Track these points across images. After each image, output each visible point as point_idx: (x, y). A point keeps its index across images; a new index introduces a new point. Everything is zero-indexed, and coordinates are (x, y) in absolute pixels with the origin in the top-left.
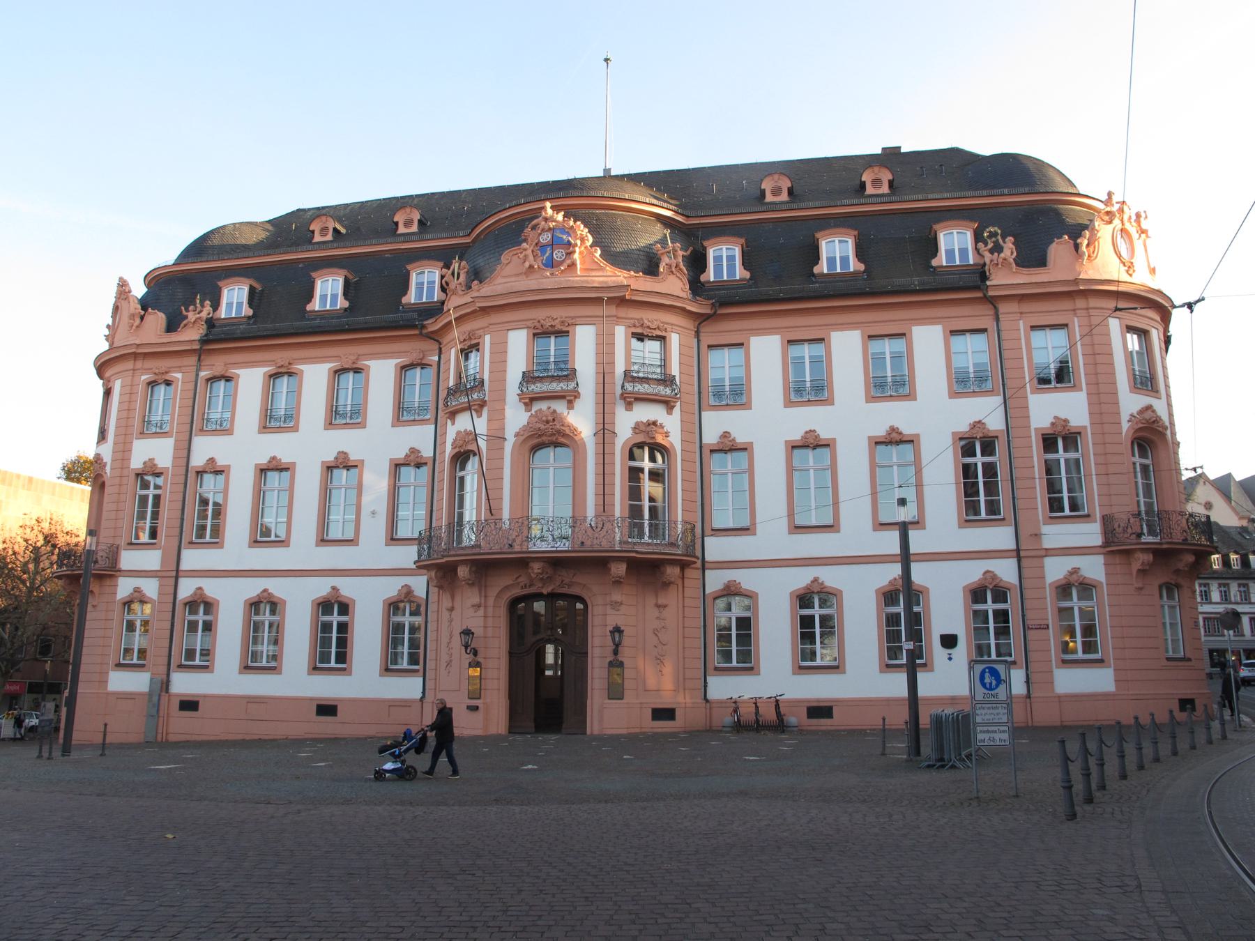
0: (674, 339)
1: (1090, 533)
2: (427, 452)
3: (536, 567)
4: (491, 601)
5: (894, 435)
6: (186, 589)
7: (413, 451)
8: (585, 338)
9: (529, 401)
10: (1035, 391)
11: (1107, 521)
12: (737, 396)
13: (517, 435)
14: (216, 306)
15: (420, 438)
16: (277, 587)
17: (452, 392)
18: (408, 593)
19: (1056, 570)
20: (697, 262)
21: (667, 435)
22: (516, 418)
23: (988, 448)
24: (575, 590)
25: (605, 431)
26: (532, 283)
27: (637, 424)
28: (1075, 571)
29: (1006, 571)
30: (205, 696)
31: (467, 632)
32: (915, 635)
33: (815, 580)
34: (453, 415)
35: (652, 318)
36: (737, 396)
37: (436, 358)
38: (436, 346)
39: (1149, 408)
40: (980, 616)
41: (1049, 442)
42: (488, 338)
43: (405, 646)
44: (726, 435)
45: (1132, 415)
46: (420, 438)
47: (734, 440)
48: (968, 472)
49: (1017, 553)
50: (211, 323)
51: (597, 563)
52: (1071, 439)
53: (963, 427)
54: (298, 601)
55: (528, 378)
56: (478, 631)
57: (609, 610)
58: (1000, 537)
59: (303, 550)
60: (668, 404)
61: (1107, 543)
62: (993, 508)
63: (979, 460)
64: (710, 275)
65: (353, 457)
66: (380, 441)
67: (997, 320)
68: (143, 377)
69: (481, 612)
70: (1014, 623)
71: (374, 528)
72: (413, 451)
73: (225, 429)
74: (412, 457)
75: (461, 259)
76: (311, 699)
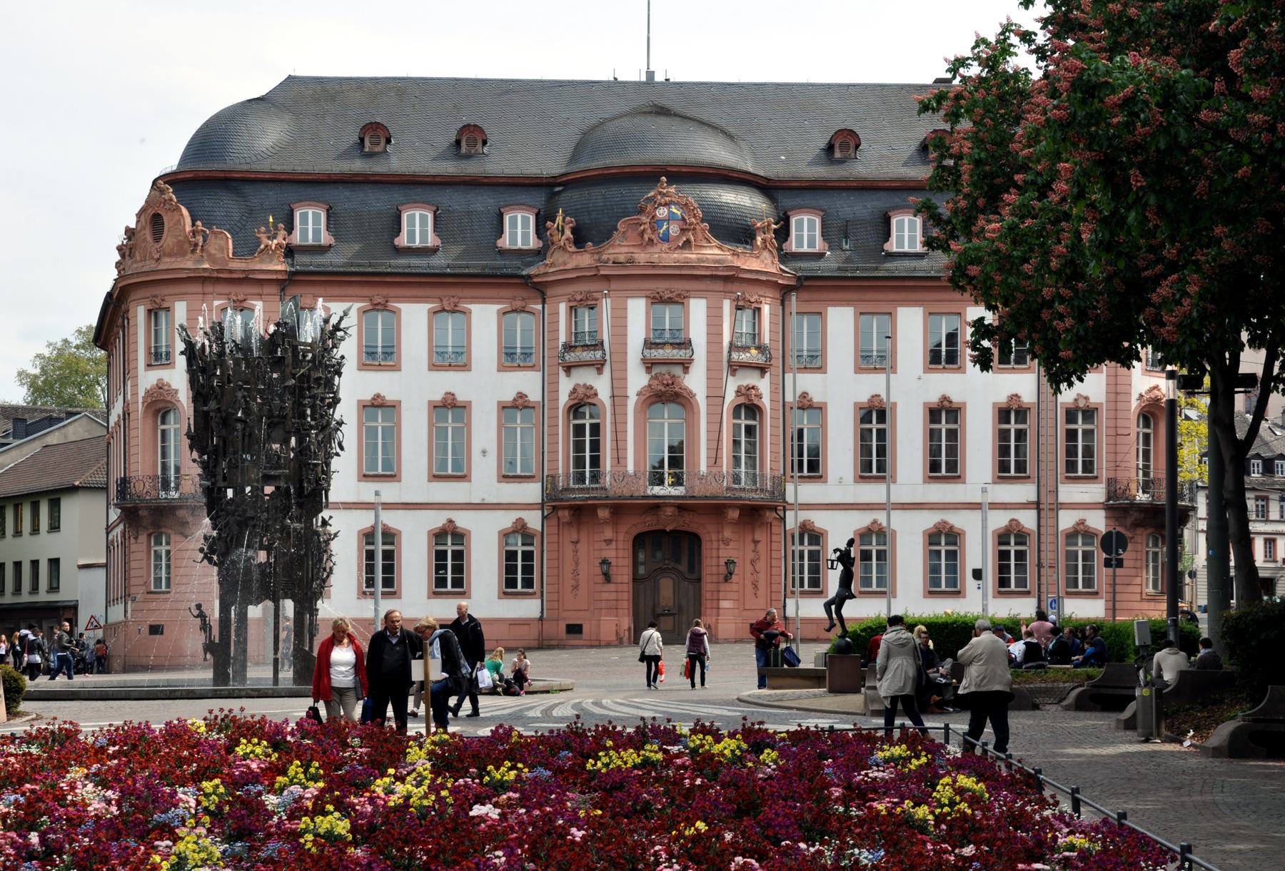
0: (766, 309)
1: (1095, 492)
2: (534, 395)
3: (669, 511)
4: (621, 537)
5: (946, 403)
7: (521, 396)
9: (649, 365)
11: (1111, 482)
12: (815, 362)
14: (290, 229)
15: (529, 383)
16: (391, 519)
17: (569, 347)
18: (520, 529)
19: (1067, 520)
20: (783, 233)
21: (759, 396)
22: (637, 380)
24: (693, 528)
25: (716, 397)
26: (642, 257)
27: (739, 387)
28: (1082, 522)
29: (1028, 520)
31: (605, 562)
32: (952, 569)
33: (875, 522)
34: (568, 369)
35: (753, 294)
36: (815, 362)
37: (539, 307)
38: (538, 294)
39: (1156, 387)
40: (1004, 556)
42: (606, 305)
43: (518, 572)
44: (804, 395)
45: (1141, 396)
46: (529, 383)
47: (810, 400)
48: (1003, 435)
49: (1037, 505)
50: (290, 252)
51: (715, 509)
53: (1002, 399)
55: (649, 344)
56: (613, 562)
57: (722, 546)
58: (1024, 492)
60: (762, 370)
61: (1109, 499)
62: (1021, 467)
63: (1013, 427)
64: (792, 246)
65: (461, 397)
66: (487, 386)
69: (613, 545)
70: (1030, 561)
71: (484, 468)
72: (521, 396)
74: (520, 401)
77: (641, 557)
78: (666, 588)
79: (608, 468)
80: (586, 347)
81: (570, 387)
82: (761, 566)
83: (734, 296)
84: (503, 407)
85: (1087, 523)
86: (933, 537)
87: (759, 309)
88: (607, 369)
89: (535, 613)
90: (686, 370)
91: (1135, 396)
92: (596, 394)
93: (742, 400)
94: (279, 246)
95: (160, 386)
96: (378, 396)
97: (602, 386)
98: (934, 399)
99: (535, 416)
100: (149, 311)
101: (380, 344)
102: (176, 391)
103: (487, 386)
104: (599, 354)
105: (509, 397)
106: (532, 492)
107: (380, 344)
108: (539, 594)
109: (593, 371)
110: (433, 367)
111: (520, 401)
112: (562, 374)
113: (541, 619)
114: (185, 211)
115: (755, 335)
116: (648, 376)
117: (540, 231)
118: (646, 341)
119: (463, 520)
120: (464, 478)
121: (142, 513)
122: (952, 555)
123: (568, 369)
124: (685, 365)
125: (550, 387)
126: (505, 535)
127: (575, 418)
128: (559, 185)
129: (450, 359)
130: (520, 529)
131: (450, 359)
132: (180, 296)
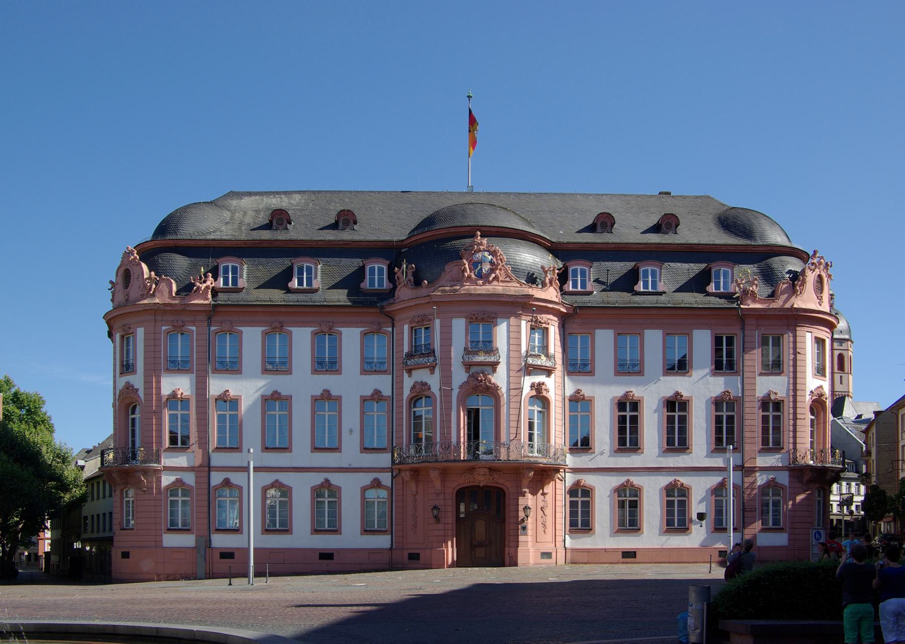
2: (387, 392)
6: (216, 478)
8: (501, 331)
9: (468, 366)
10: (761, 374)
13: (461, 387)
14: (215, 278)
15: (383, 383)
17: (410, 356)
22: (459, 376)
23: (731, 407)
28: (773, 479)
30: (238, 549)
31: (435, 508)
34: (410, 372)
37: (390, 329)
39: (821, 387)
41: (765, 403)
45: (812, 392)
50: (215, 292)
52: (778, 405)
54: (302, 488)
59: (301, 454)
65: (334, 393)
66: (352, 384)
67: (743, 329)
68: (164, 328)
69: (442, 496)
71: (351, 442)
73: (233, 368)
75: (409, 263)
76: (316, 550)
77: (462, 508)
78: (480, 527)
79: (438, 440)
80: (423, 355)
81: (412, 384)
82: (549, 511)
83: (529, 318)
84: (364, 400)
85: (777, 480)
86: (670, 490)
87: (547, 329)
88: (437, 370)
89: (387, 545)
90: (494, 371)
91: (808, 393)
92: (429, 388)
93: (534, 393)
94: (207, 287)
95: (129, 387)
96: (276, 392)
97: (434, 381)
98: (669, 393)
99: (385, 405)
100: (122, 337)
101: (277, 355)
102: (137, 390)
103: (352, 384)
104: (431, 359)
105: (368, 392)
106: (384, 460)
107: (277, 355)
108: (389, 531)
109: (427, 371)
110: (315, 371)
111: (376, 396)
112: (406, 375)
113: (391, 549)
114: (144, 266)
115: (545, 348)
116: (467, 375)
117: (391, 276)
118: (465, 349)
119: (336, 479)
120: (337, 449)
121: (115, 475)
122: (682, 504)
123: (410, 372)
124: (494, 365)
125: (397, 385)
126: (364, 489)
127: (415, 407)
128: (405, 247)
129: (327, 364)
130: (377, 484)
131: (327, 364)
132: (140, 324)
